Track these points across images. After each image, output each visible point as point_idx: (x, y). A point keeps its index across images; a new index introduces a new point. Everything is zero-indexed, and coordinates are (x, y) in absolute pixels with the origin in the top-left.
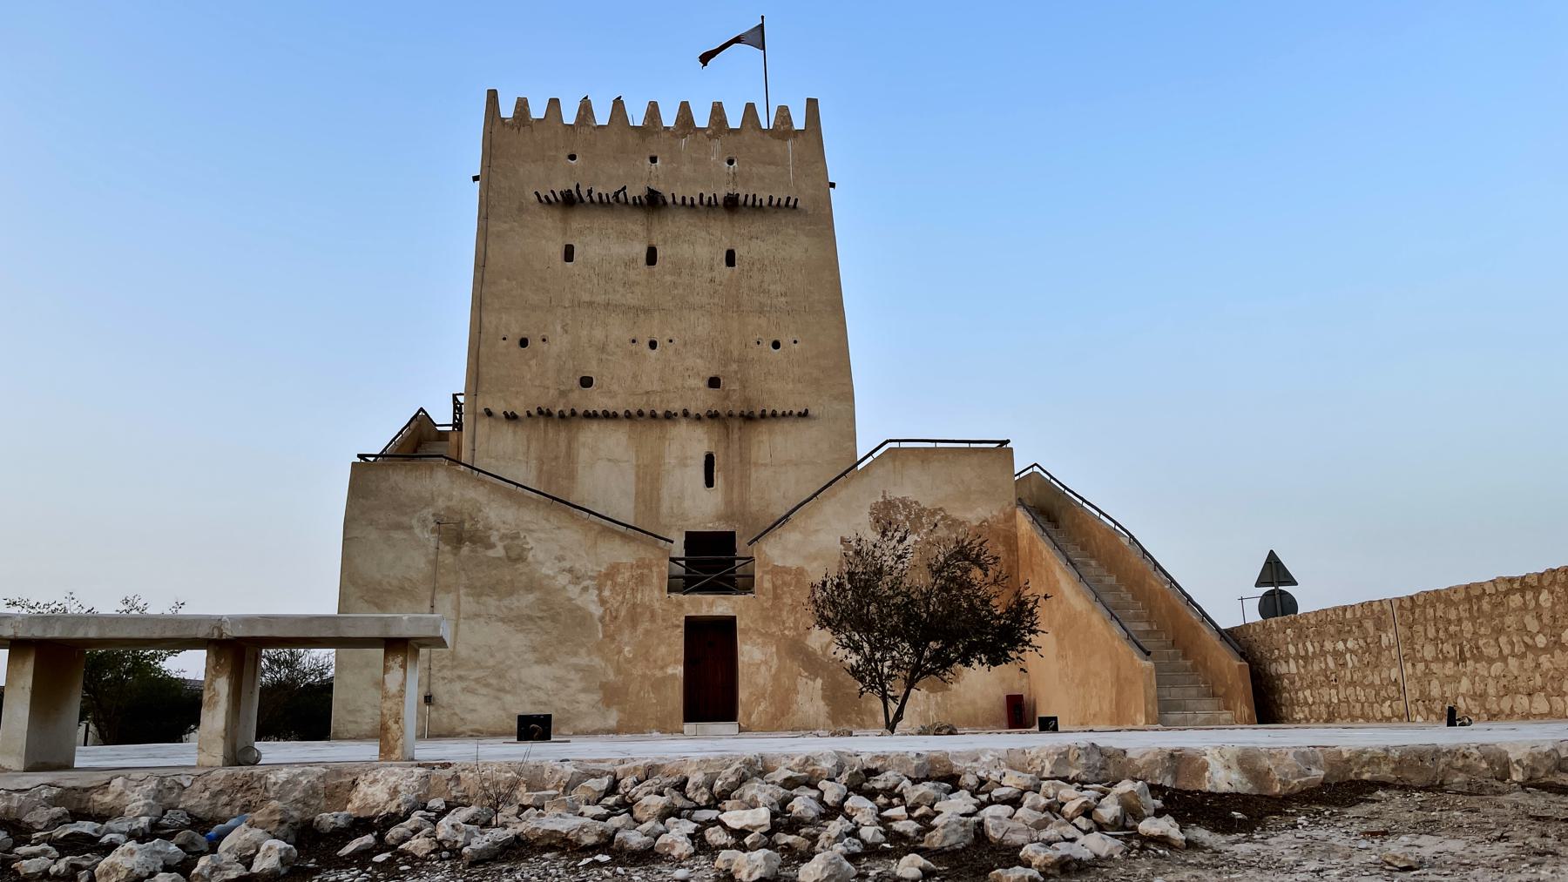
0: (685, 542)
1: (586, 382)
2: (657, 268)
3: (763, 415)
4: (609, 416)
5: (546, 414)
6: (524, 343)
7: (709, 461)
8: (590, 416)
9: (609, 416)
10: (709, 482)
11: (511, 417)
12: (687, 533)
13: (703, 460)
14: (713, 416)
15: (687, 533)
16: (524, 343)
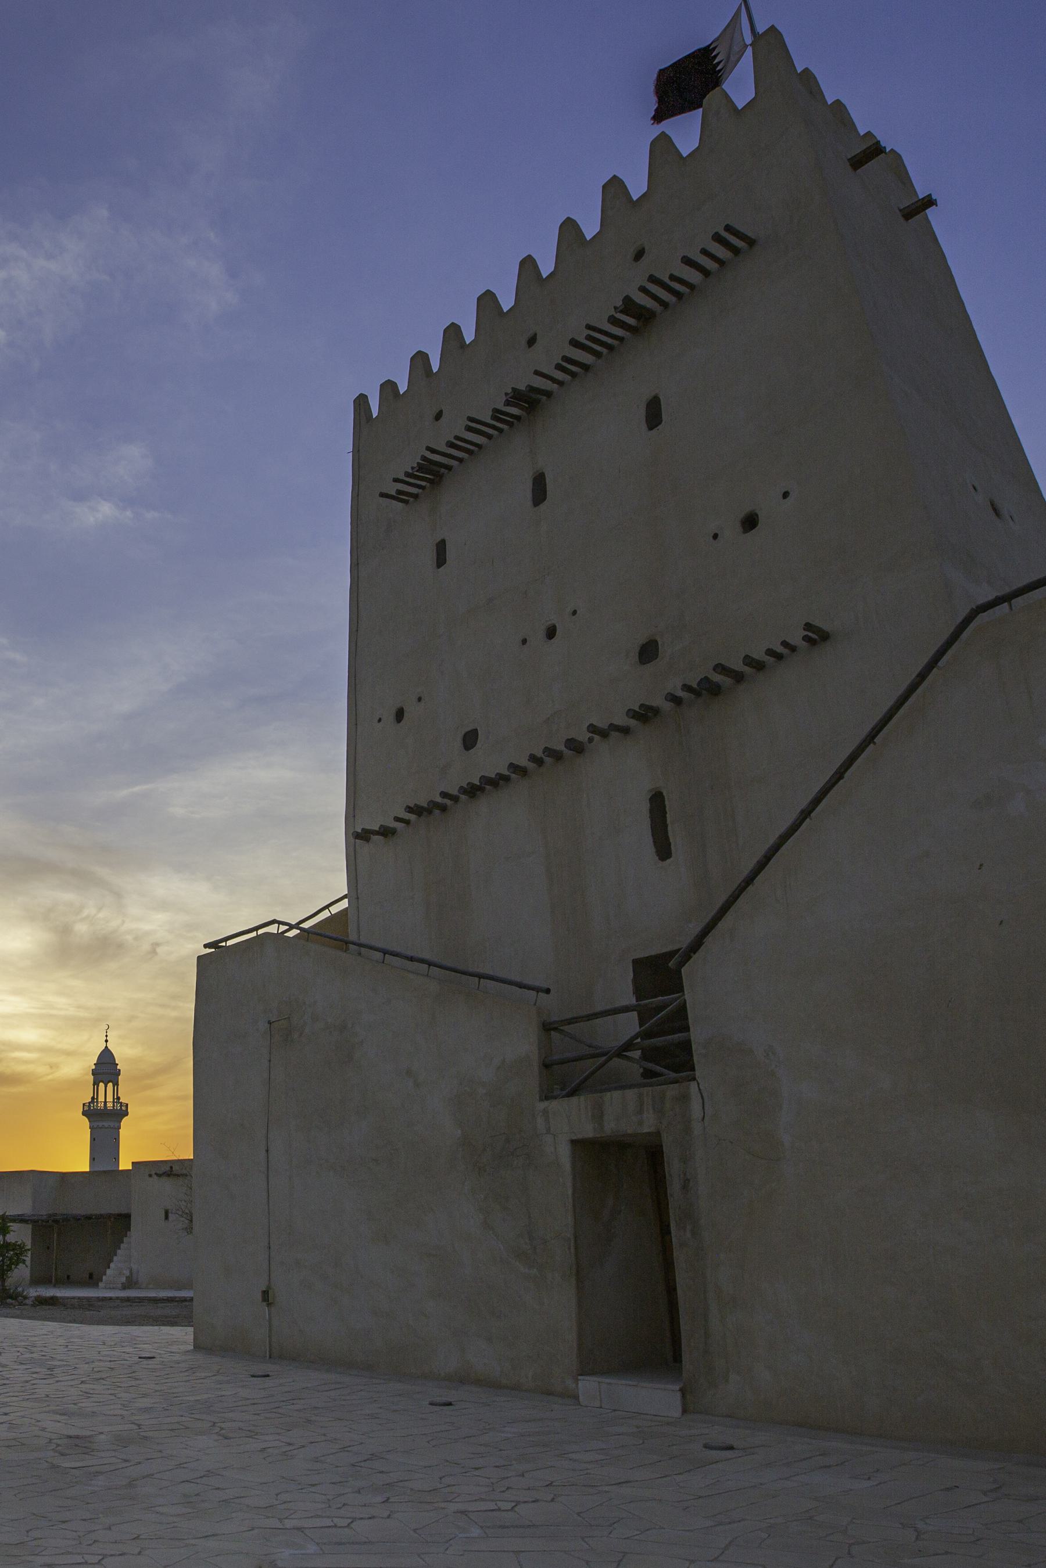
0: (635, 981)
1: (470, 740)
2: (543, 507)
3: (739, 677)
4: (497, 782)
5: (417, 810)
6: (400, 715)
7: (657, 801)
8: (473, 791)
9: (497, 782)
10: (664, 850)
11: (386, 832)
12: (636, 962)
13: (645, 807)
14: (645, 714)
15: (636, 962)
16: (400, 715)
